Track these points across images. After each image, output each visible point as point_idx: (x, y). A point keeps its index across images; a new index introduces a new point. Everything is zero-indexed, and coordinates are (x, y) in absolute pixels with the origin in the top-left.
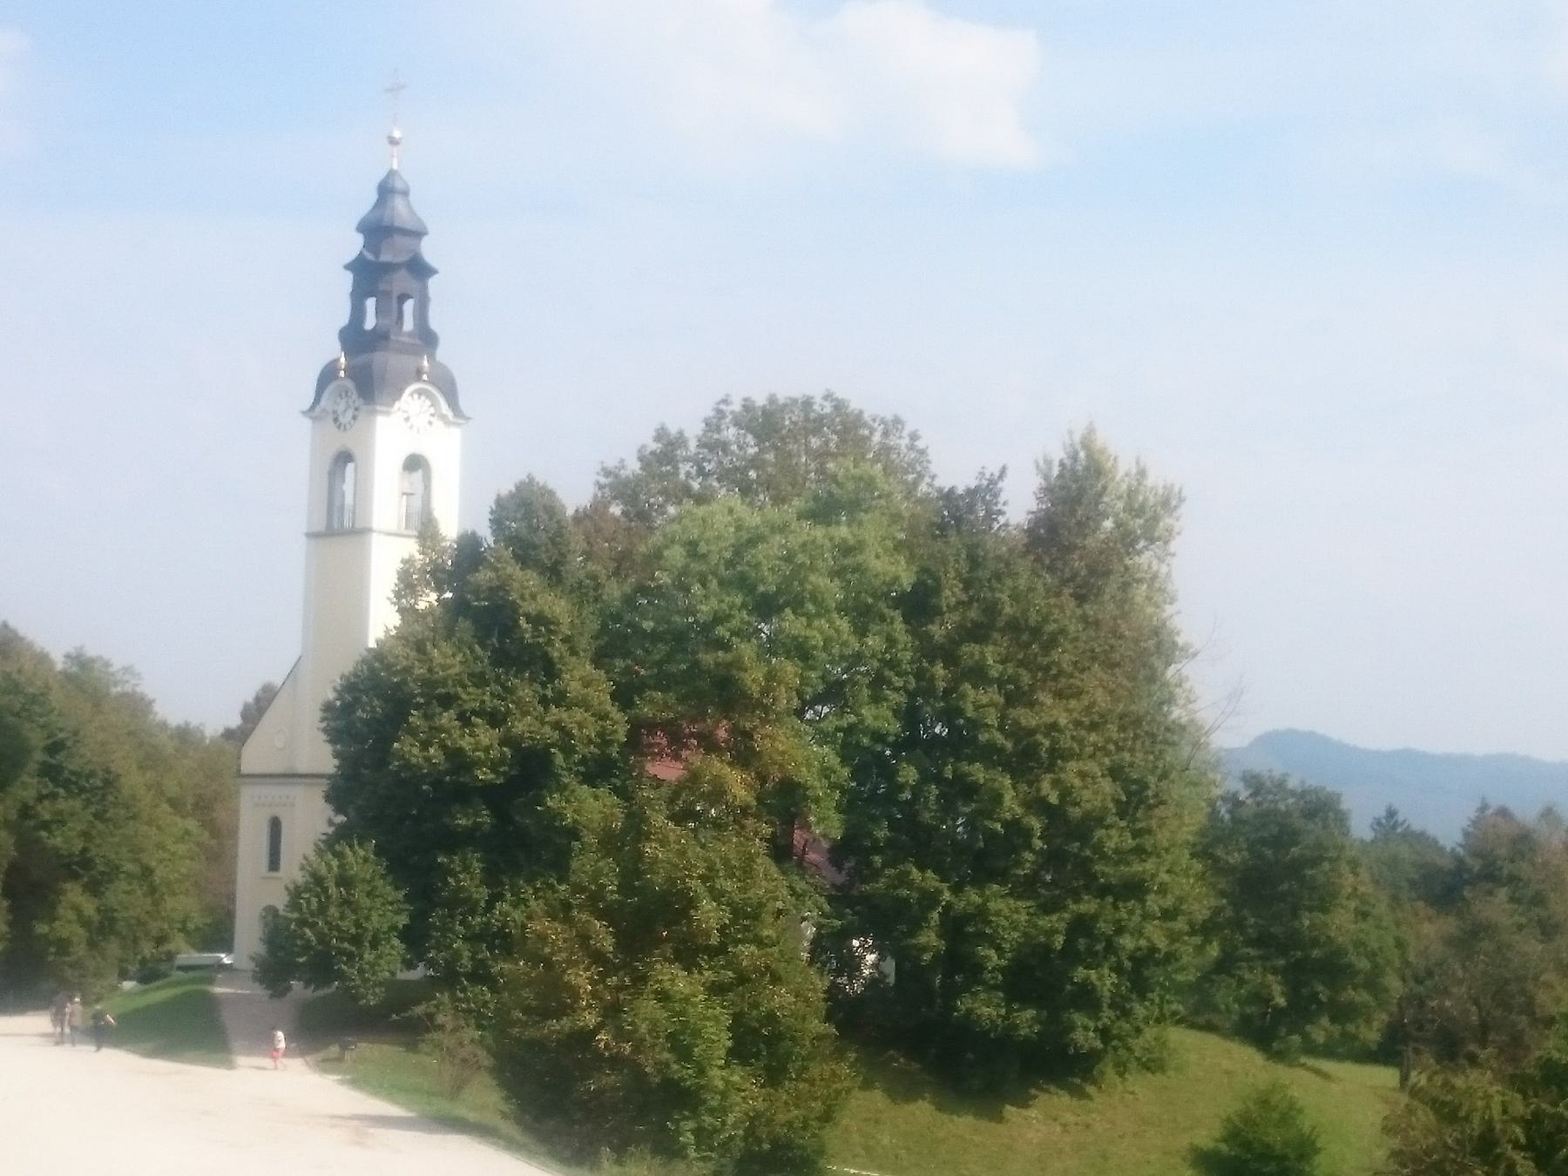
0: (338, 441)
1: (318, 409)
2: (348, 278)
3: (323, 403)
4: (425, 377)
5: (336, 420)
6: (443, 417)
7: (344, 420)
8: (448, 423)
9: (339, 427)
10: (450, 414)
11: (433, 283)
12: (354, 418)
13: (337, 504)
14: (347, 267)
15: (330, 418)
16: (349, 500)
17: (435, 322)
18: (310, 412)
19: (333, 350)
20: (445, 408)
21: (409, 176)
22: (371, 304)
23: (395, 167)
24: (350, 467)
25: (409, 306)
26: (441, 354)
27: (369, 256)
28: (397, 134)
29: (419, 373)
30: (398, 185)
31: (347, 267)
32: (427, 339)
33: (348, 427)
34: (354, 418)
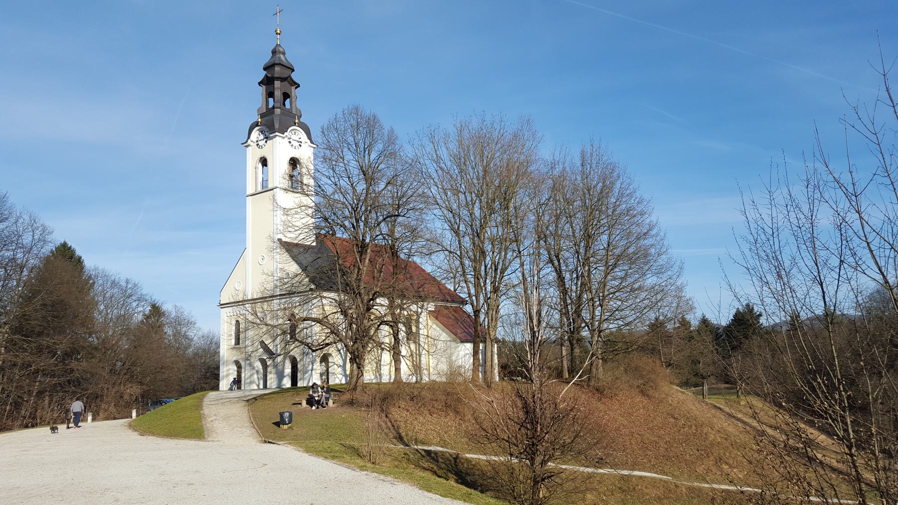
0: (260, 153)
1: (249, 141)
4: (297, 125)
5: (258, 145)
7: (260, 143)
10: (308, 141)
14: (260, 83)
15: (255, 144)
20: (304, 138)
21: (285, 47)
25: (288, 102)
26: (301, 120)
27: (269, 75)
30: (282, 50)
33: (263, 146)
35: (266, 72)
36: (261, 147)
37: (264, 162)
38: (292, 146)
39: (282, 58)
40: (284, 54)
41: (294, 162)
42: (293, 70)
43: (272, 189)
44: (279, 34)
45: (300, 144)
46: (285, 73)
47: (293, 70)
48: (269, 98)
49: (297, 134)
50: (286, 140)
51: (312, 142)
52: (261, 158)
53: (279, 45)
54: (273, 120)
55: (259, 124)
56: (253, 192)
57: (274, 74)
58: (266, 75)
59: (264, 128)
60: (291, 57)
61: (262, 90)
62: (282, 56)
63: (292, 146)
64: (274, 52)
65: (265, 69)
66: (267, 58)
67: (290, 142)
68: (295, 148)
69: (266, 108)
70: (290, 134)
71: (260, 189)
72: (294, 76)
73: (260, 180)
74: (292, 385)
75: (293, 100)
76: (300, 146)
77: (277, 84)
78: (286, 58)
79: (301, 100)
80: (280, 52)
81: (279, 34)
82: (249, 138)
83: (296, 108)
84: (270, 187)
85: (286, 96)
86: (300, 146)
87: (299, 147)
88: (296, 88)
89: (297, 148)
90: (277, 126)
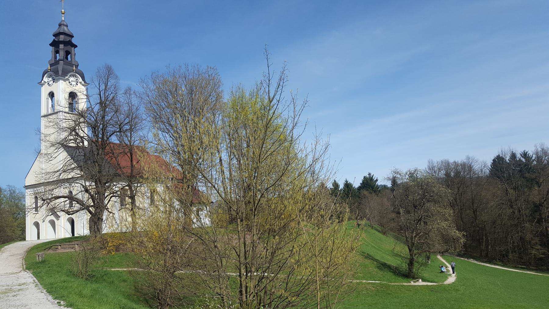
1: (43, 81)
3: (44, 80)
4: (74, 71)
5: (48, 84)
6: (80, 83)
8: (83, 85)
9: (49, 86)
10: (83, 82)
12: (54, 82)
14: (51, 45)
15: (47, 83)
21: (67, 22)
23: (63, 19)
25: (69, 57)
26: (79, 68)
27: (56, 40)
28: (63, 11)
30: (65, 23)
31: (51, 45)
33: (52, 85)
35: (54, 38)
36: (50, 85)
38: (71, 84)
39: (65, 29)
40: (67, 26)
41: (73, 95)
43: (57, 113)
44: (64, 14)
45: (77, 83)
46: (68, 39)
48: (57, 53)
51: (85, 82)
52: (50, 92)
53: (64, 20)
54: (58, 68)
55: (49, 70)
56: (46, 114)
57: (59, 39)
58: (54, 40)
59: (51, 73)
60: (71, 29)
61: (51, 49)
62: (65, 28)
64: (60, 25)
65: (54, 36)
67: (69, 82)
69: (55, 60)
71: (50, 111)
72: (74, 41)
73: (50, 106)
74: (72, 236)
75: (73, 56)
76: (77, 84)
77: (61, 46)
78: (68, 29)
80: (64, 25)
81: (64, 14)
82: (42, 80)
83: (75, 61)
84: (56, 111)
85: (68, 53)
86: (77, 84)
87: (76, 85)
88: (75, 48)
89: (74, 86)
90: (60, 72)
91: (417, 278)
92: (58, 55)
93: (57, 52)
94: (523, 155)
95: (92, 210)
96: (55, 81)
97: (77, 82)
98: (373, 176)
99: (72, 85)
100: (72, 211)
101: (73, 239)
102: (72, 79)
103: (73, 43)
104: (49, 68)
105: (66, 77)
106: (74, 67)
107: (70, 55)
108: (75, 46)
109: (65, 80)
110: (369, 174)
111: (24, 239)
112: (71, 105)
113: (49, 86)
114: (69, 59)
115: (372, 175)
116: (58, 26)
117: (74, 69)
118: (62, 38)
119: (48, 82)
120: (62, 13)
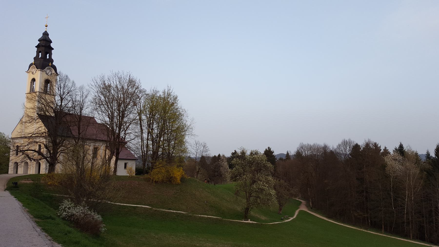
0: (32, 77)
1: (29, 71)
2: (36, 48)
4: (50, 66)
5: (32, 73)
9: (33, 74)
10: (55, 73)
11: (52, 51)
12: (36, 72)
13: (32, 88)
14: (36, 47)
15: (31, 73)
16: (34, 87)
17: (53, 57)
18: (28, 72)
19: (33, 61)
20: (54, 72)
22: (40, 54)
23: (46, 30)
24: (35, 82)
25: (48, 55)
26: (54, 64)
29: (49, 66)
31: (36, 47)
32: (52, 61)
34: (36, 72)
35: (39, 42)
37: (34, 80)
40: (48, 35)
41: (47, 82)
42: (52, 42)
47: (52, 42)
49: (50, 70)
50: (45, 73)
52: (33, 79)
55: (33, 64)
59: (34, 66)
62: (47, 36)
63: (47, 75)
64: (43, 34)
65: (39, 41)
66: (40, 36)
67: (46, 73)
68: (49, 76)
70: (47, 70)
72: (52, 45)
73: (32, 88)
78: (48, 37)
79: (55, 55)
81: (47, 27)
82: (29, 69)
84: (36, 91)
89: (49, 75)
91: (248, 218)
92: (40, 54)
93: (40, 52)
94: (374, 144)
95: (49, 160)
96: (37, 71)
97: (52, 73)
98: (271, 149)
99: (48, 75)
100: (37, 160)
101: (38, 176)
102: (48, 71)
103: (51, 46)
104: (33, 63)
105: (44, 70)
106: (50, 63)
107: (48, 54)
108: (53, 49)
109: (43, 71)
110: (269, 148)
111: (7, 172)
112: (46, 88)
113: (33, 74)
114: (48, 57)
115: (270, 148)
116: (42, 35)
117: (50, 64)
118: (43, 43)
119: (32, 71)
120: (46, 26)
